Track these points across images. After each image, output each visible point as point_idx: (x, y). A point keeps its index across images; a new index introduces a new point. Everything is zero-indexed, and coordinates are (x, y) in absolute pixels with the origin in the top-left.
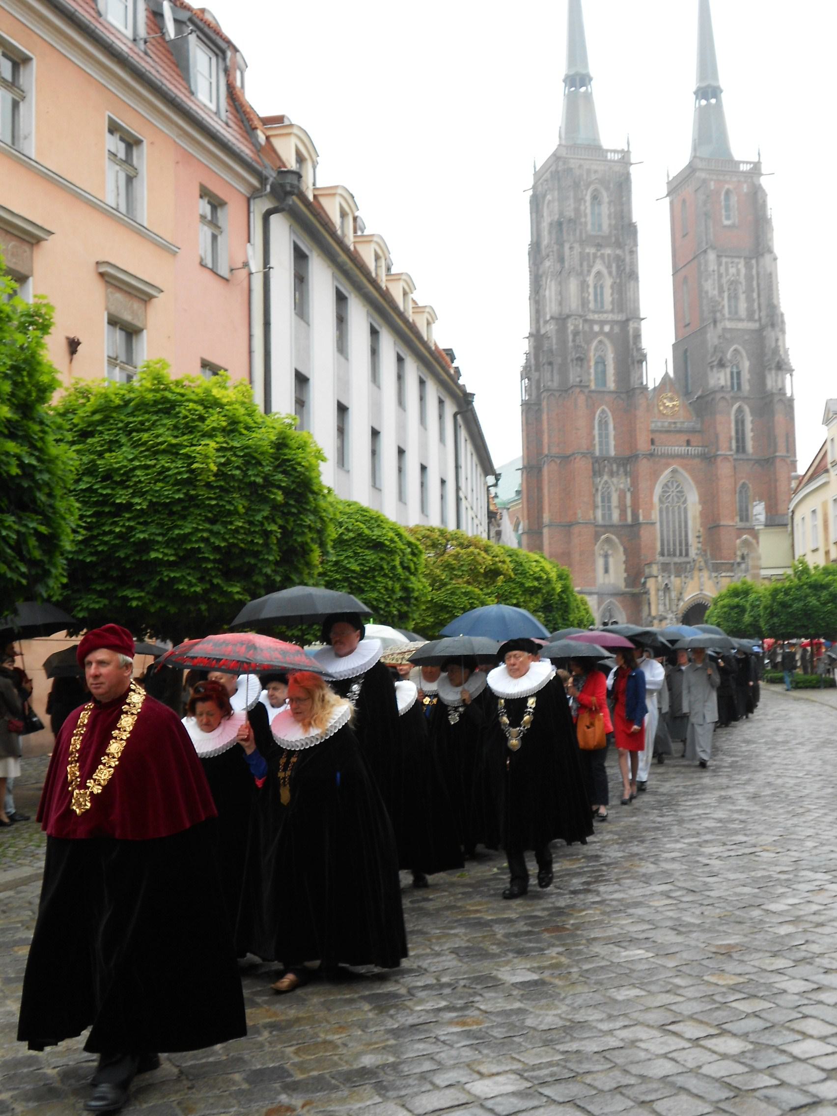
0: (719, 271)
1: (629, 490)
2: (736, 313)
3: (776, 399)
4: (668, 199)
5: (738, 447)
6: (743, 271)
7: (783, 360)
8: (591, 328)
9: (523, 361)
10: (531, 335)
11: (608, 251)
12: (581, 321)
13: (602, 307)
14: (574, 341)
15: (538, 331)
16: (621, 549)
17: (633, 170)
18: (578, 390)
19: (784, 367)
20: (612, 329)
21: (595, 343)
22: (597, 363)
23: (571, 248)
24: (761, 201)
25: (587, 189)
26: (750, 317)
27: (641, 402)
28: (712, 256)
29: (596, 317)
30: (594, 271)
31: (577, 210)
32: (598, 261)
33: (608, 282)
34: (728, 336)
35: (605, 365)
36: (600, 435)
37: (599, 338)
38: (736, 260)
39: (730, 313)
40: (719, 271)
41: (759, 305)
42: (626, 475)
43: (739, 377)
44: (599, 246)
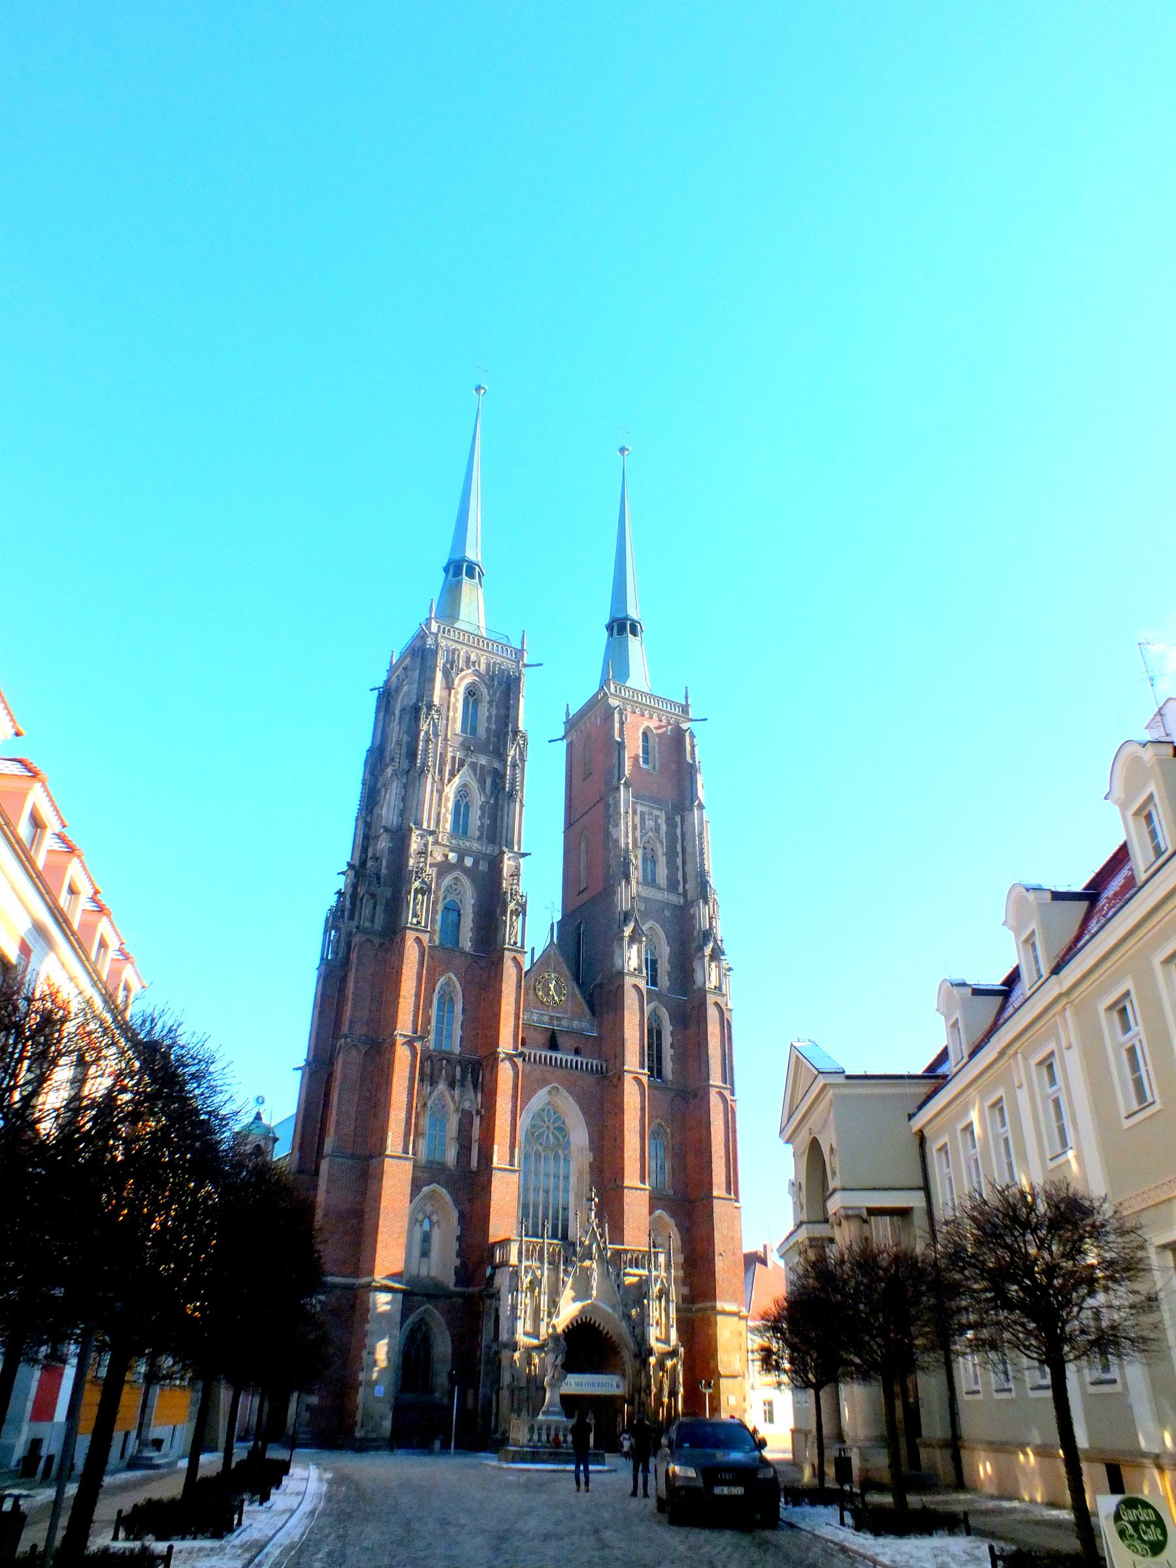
1: (478, 1112)
2: (654, 880)
3: (711, 999)
4: (564, 743)
6: (664, 827)
9: (332, 900)
15: (363, 863)
16: (455, 1215)
17: (524, 670)
20: (476, 863)
22: (446, 908)
23: (427, 741)
25: (462, 679)
35: (459, 915)
36: (440, 1020)
37: (456, 874)
38: (656, 812)
41: (684, 874)
42: (475, 1087)
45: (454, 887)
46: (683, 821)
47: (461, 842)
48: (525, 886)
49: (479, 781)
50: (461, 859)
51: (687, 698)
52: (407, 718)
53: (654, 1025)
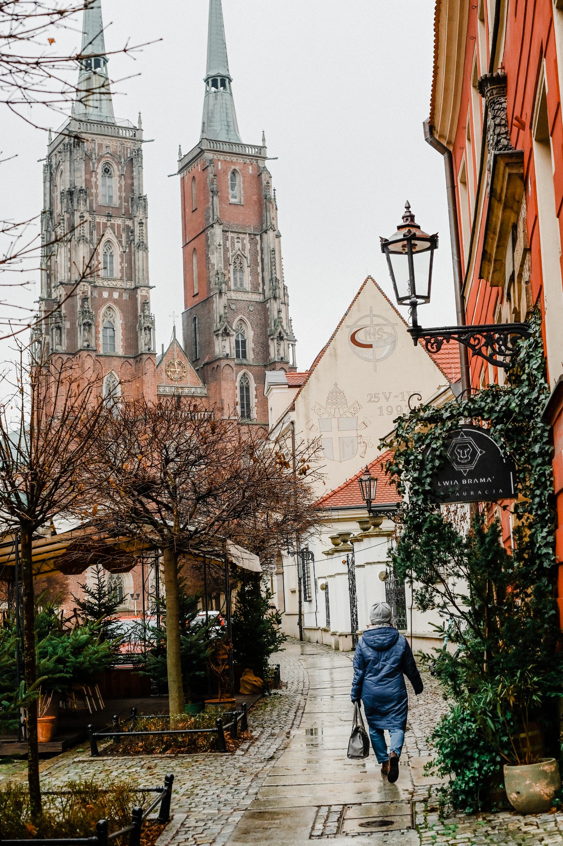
0: (225, 245)
2: (242, 285)
4: (179, 177)
5: (243, 412)
6: (248, 246)
7: (285, 331)
8: (100, 295)
10: (42, 299)
11: (118, 221)
12: (90, 287)
13: (112, 275)
14: (82, 306)
17: (144, 146)
18: (85, 354)
19: (285, 337)
20: (120, 296)
21: (103, 310)
24: (264, 183)
26: (255, 290)
27: (149, 367)
28: (218, 230)
29: (106, 283)
30: (104, 239)
31: (87, 181)
32: (109, 231)
33: (117, 251)
34: (233, 307)
37: (108, 305)
38: (241, 236)
39: (235, 284)
40: (225, 245)
41: (263, 278)
43: (244, 346)
44: (109, 216)
45: (108, 313)
46: (261, 239)
47: (109, 282)
48: (154, 309)
49: (117, 237)
50: (111, 295)
51: (264, 140)
52: (65, 201)
53: (245, 384)
